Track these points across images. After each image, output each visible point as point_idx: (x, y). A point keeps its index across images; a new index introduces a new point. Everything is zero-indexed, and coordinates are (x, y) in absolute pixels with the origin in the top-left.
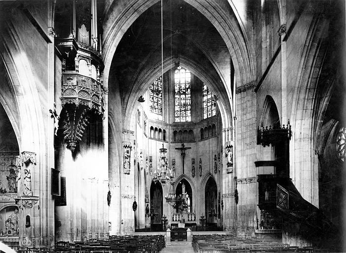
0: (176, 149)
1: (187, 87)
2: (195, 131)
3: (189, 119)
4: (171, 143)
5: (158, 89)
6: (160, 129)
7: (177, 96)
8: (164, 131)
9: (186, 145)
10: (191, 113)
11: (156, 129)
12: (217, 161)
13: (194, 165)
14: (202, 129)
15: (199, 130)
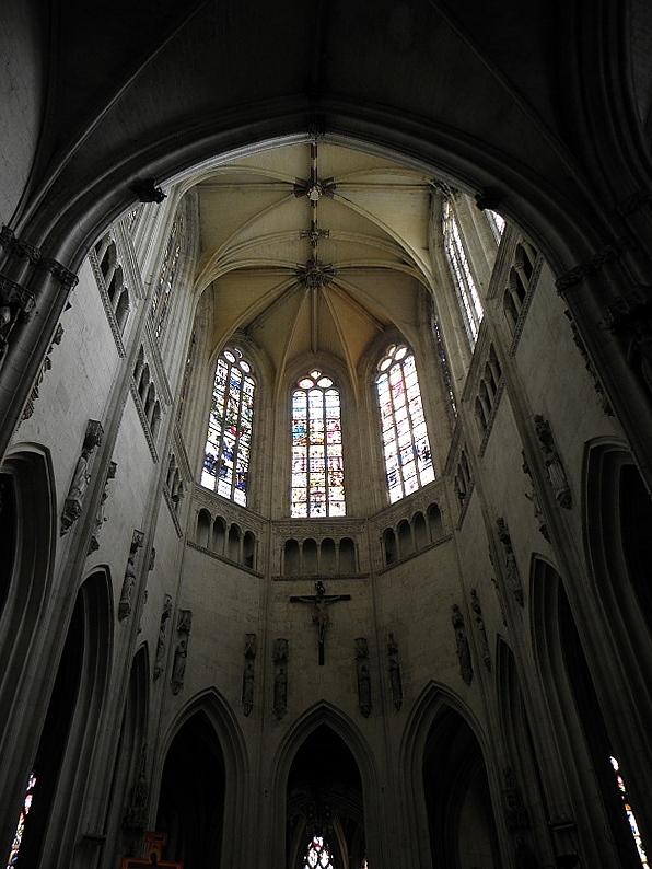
0: (294, 600)
2: (361, 542)
3: (338, 511)
4: (277, 579)
6: (234, 529)
7: (294, 450)
8: (249, 538)
9: (332, 588)
10: (345, 492)
14: (389, 534)
15: (378, 534)
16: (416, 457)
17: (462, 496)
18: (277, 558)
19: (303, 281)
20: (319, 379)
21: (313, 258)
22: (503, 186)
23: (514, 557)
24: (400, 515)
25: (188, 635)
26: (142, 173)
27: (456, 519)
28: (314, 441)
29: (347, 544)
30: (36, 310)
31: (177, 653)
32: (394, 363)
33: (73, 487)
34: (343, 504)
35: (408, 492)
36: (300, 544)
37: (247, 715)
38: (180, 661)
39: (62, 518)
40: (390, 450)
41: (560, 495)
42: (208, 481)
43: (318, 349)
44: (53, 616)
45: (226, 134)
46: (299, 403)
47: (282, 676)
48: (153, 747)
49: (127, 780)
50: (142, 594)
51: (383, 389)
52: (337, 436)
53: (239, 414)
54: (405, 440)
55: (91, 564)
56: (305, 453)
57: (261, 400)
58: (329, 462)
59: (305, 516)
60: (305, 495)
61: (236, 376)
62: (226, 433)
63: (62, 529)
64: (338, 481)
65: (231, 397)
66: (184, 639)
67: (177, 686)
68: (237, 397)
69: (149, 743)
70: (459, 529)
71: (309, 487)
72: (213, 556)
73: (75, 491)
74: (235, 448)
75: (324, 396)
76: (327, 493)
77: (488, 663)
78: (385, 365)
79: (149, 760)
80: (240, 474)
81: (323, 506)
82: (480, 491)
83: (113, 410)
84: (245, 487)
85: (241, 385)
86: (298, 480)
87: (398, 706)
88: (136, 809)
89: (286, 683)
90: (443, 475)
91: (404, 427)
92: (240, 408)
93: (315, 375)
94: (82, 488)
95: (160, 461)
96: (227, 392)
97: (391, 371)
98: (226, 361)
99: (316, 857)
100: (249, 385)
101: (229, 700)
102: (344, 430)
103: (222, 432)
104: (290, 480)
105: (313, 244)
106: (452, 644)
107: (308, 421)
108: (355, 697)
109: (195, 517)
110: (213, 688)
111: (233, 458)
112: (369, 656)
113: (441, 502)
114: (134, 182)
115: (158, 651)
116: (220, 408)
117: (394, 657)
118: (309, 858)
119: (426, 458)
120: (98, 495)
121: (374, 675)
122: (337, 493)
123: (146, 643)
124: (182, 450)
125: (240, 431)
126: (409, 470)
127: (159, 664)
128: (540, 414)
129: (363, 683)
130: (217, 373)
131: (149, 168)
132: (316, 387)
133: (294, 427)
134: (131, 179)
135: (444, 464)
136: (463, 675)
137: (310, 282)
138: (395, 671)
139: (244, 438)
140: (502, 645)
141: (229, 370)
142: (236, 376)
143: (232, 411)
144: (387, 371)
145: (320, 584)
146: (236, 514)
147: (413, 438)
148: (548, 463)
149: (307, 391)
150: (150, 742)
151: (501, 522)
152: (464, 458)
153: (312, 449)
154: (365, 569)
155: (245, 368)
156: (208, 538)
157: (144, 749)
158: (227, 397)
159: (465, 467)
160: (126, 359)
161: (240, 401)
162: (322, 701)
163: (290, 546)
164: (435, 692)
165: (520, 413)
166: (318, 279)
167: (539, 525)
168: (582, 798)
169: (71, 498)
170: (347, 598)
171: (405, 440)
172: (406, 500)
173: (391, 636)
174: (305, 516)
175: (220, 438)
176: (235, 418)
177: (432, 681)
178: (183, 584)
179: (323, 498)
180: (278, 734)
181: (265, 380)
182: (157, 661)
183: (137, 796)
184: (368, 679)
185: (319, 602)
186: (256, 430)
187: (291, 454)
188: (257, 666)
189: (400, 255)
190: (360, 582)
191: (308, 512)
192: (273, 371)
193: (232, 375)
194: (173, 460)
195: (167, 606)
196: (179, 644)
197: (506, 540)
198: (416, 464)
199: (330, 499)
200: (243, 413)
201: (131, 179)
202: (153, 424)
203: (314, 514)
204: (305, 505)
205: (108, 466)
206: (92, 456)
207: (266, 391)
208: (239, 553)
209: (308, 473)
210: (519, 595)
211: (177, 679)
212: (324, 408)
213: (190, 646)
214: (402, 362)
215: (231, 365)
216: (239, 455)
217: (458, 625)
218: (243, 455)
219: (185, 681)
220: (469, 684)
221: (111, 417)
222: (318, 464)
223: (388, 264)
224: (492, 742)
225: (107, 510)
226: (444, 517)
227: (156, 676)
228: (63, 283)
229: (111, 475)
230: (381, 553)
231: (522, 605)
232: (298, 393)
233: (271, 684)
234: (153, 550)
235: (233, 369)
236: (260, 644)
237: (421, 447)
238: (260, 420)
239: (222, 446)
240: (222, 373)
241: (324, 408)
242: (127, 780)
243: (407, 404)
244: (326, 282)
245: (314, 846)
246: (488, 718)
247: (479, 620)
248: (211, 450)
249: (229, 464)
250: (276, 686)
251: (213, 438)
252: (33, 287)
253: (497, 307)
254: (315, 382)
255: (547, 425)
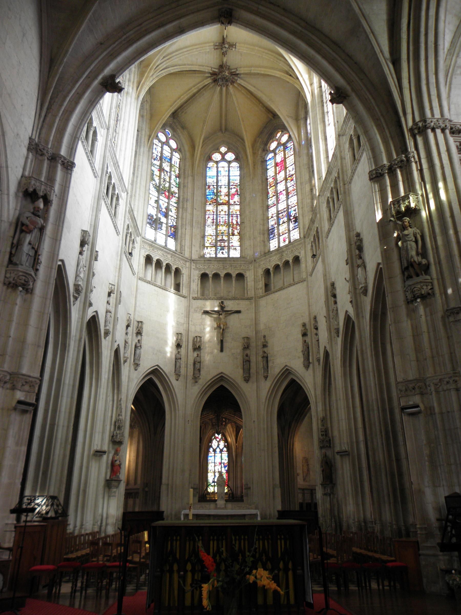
1: (233, 191)
2: (249, 276)
3: (235, 254)
4: (194, 299)
5: (170, 187)
6: (168, 267)
8: (177, 271)
9: (230, 305)
10: (241, 240)
11: (159, 264)
12: (308, 339)
13: (248, 352)
14: (267, 272)
15: (260, 272)
16: (289, 220)
17: (314, 256)
18: (196, 285)
19: (215, 81)
20: (226, 153)
21: (224, 39)
22: (348, 88)
23: (337, 307)
24: (275, 260)
25: (141, 335)
26: (107, 71)
27: (310, 269)
28: (221, 202)
29: (240, 276)
30: (55, 194)
31: (136, 347)
32: (279, 144)
33: (77, 276)
34: (239, 248)
35: (282, 244)
36: (210, 276)
37: (177, 380)
38: (138, 351)
39: (74, 296)
40: (272, 211)
41: (362, 287)
42: (150, 233)
43: (226, 129)
44: (74, 350)
45: (162, 30)
46: (211, 172)
47: (198, 359)
48: (125, 399)
49: (112, 417)
50: (116, 319)
51: (270, 164)
52: (236, 198)
53: (170, 182)
54: (282, 206)
55: (90, 313)
56: (215, 210)
57: (184, 170)
58: (231, 218)
59: (214, 256)
60: (214, 241)
61: (167, 152)
62: (161, 197)
63: (74, 302)
64: (236, 232)
65: (163, 169)
66: (139, 337)
67: (137, 365)
68: (167, 169)
69: (122, 397)
70: (311, 275)
71: (217, 235)
72: (155, 285)
73: (78, 278)
74: (167, 209)
75: (229, 167)
76: (229, 240)
77: (319, 360)
78: (273, 145)
79: (123, 406)
80: (171, 226)
81: (226, 250)
82: (323, 261)
83: (94, 217)
84: (174, 235)
85: (171, 159)
86: (210, 230)
87: (266, 377)
88: (118, 432)
89: (200, 362)
90: (304, 237)
91: (283, 197)
92: (170, 177)
93: (223, 150)
94: (82, 275)
95: (121, 233)
96: (161, 166)
97: (277, 151)
98: (160, 141)
99: (217, 444)
100: (176, 158)
101: (167, 372)
102: (241, 195)
103: (158, 197)
104: (204, 231)
105: (224, 54)
106: (300, 346)
107: (217, 186)
108: (241, 371)
109: (143, 261)
110: (157, 365)
111: (166, 215)
112: (250, 348)
113: (302, 256)
114: (103, 78)
115: (125, 347)
116: (157, 179)
117: (265, 349)
118: (213, 445)
119: (296, 221)
120: (90, 274)
121: (253, 359)
122: (235, 241)
123: (118, 345)
124: (133, 219)
125: (170, 194)
126: (283, 228)
127: (126, 355)
128: (359, 231)
129: (247, 361)
130: (154, 151)
131: (112, 66)
132: (223, 159)
133: (207, 191)
134: (100, 77)
135: (306, 230)
136: (304, 364)
137: (220, 83)
138: (266, 358)
139: (174, 200)
140: (327, 354)
141: (162, 147)
142: (167, 152)
143: (164, 180)
144: (274, 151)
145: (222, 302)
146: (169, 256)
147: (288, 206)
148: (358, 266)
149: (217, 162)
150: (123, 397)
151: (333, 285)
152: (317, 232)
153: (220, 208)
154: (251, 293)
155: (173, 144)
156: (151, 270)
157: (120, 401)
158: (161, 169)
159: (317, 237)
160: (99, 179)
161: (170, 172)
162: (222, 373)
163: (204, 276)
164: (287, 372)
165: (349, 226)
166: (227, 81)
167: (349, 299)
168: (355, 440)
169: (76, 283)
170: (238, 312)
171: (282, 206)
172: (279, 249)
173: (264, 337)
174: (214, 256)
175: (157, 202)
176: (167, 185)
177: (286, 366)
178: (137, 305)
179: (226, 244)
180: (195, 390)
181: (188, 154)
182: (125, 353)
183: (118, 425)
184: (249, 361)
185: (221, 314)
186: (181, 194)
187: (205, 212)
188: (183, 350)
189: (286, 68)
190: (247, 302)
191: (216, 254)
192: (193, 147)
193: (164, 152)
194: (128, 227)
195: (129, 320)
196: (137, 341)
197: (334, 296)
198: (289, 225)
199: (231, 245)
200: (172, 181)
201: (100, 77)
202: (116, 208)
203: (220, 255)
204: (214, 249)
205: (94, 253)
206: (85, 253)
207: (188, 164)
208: (171, 279)
209: (217, 225)
210: (337, 330)
211: (137, 362)
212: (229, 176)
213: (144, 343)
214: (285, 146)
215: (163, 144)
216: (170, 213)
217: (304, 335)
218: (173, 213)
219: (141, 363)
220: (307, 370)
221: (93, 223)
222: (223, 218)
223: (278, 74)
224: (316, 403)
225: (95, 281)
226: (303, 265)
227: (125, 361)
228: (67, 169)
229: (96, 259)
230: (261, 284)
231: (338, 336)
232: (210, 164)
233: (191, 362)
234: (120, 292)
235: (165, 147)
236: (184, 339)
237: (293, 213)
238: (184, 186)
239: (158, 208)
240: (157, 151)
241: (229, 176)
242: (112, 417)
243: (286, 179)
244: (233, 82)
245: (216, 438)
246: (315, 390)
247: (316, 334)
248: (153, 211)
249: (163, 220)
250: (194, 364)
251: (152, 202)
252: (51, 179)
253: (345, 143)
254: (223, 155)
255: (361, 240)
